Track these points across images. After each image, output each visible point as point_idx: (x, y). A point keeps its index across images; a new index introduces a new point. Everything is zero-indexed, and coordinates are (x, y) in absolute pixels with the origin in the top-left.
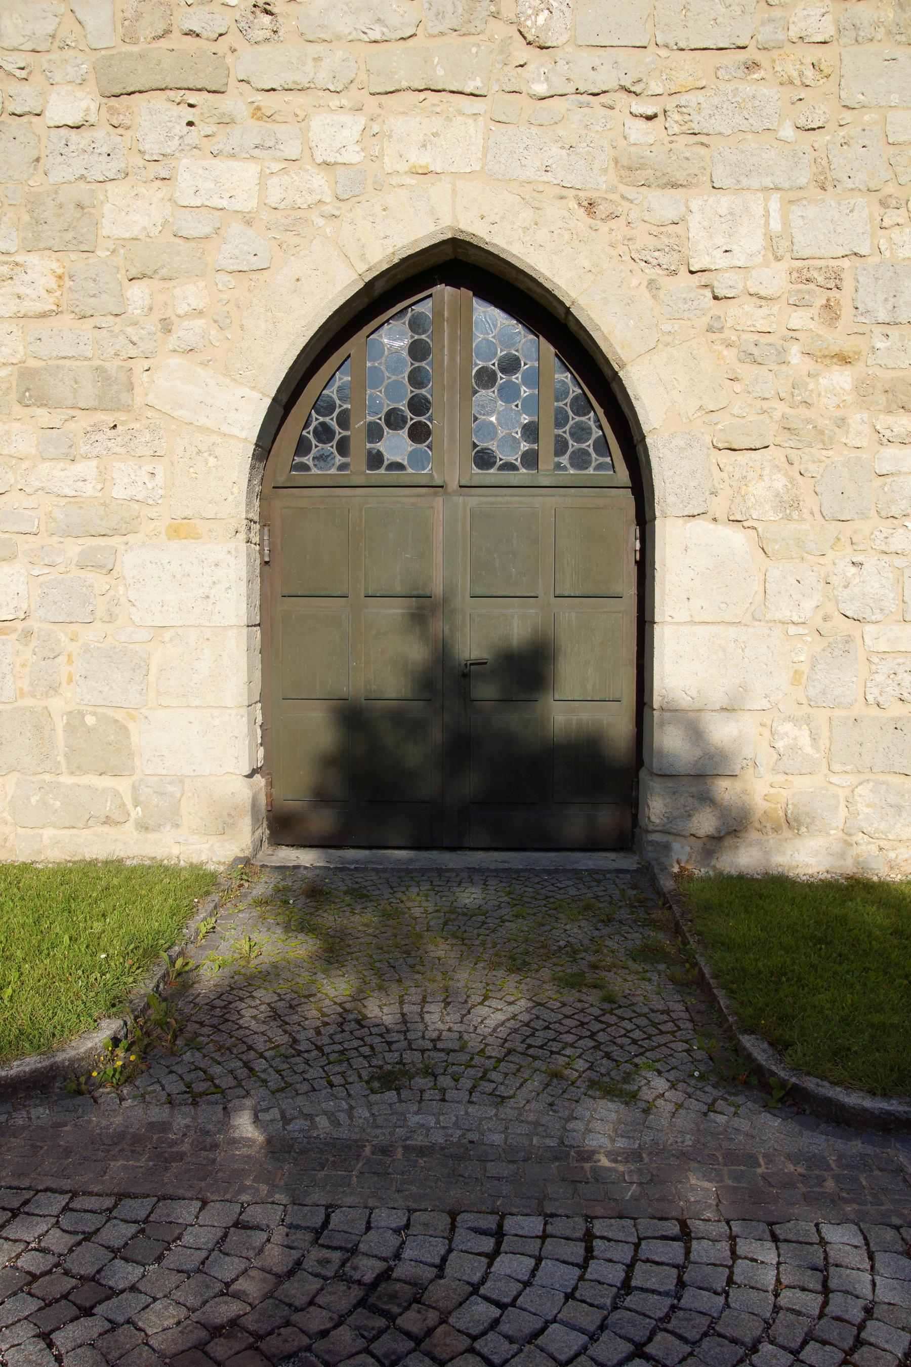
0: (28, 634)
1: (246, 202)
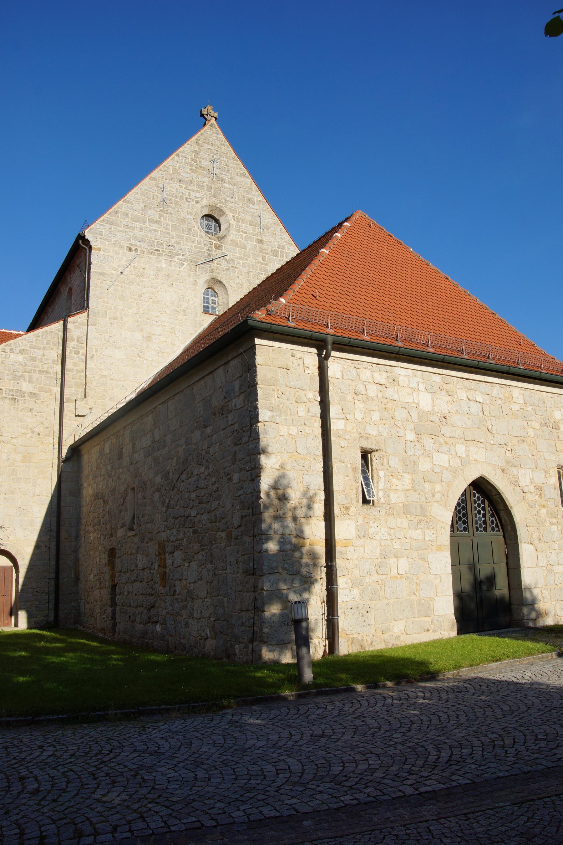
0: (408, 578)
1: (447, 465)
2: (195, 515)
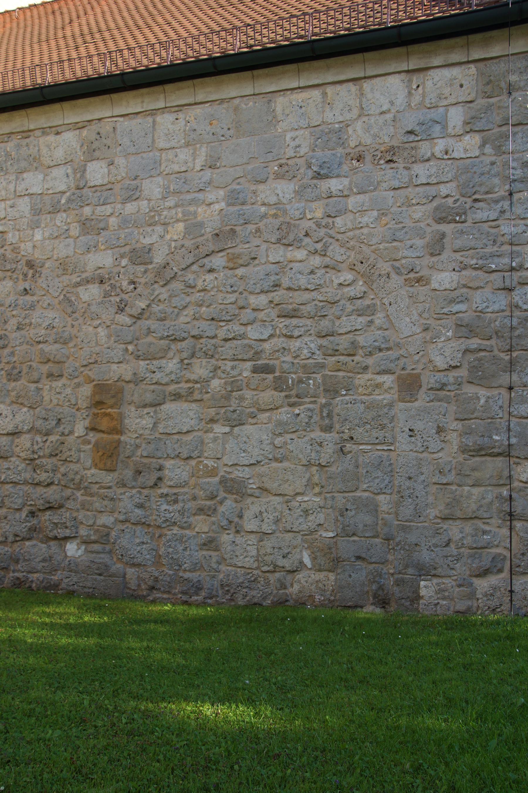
2: (265, 337)
